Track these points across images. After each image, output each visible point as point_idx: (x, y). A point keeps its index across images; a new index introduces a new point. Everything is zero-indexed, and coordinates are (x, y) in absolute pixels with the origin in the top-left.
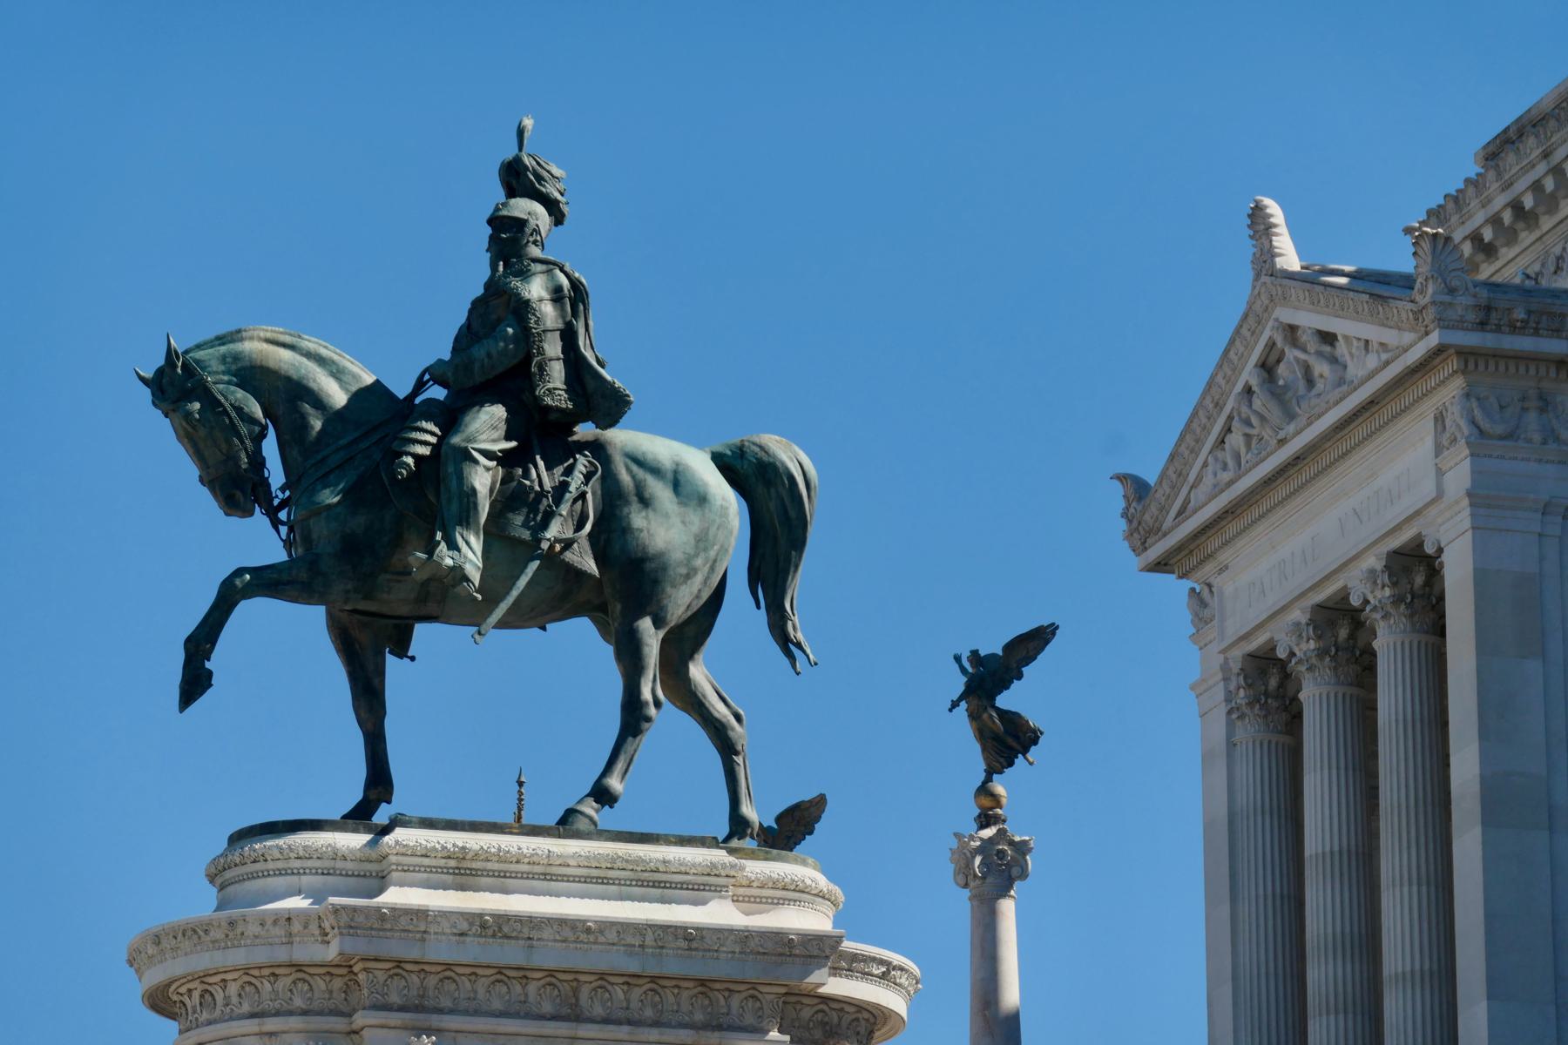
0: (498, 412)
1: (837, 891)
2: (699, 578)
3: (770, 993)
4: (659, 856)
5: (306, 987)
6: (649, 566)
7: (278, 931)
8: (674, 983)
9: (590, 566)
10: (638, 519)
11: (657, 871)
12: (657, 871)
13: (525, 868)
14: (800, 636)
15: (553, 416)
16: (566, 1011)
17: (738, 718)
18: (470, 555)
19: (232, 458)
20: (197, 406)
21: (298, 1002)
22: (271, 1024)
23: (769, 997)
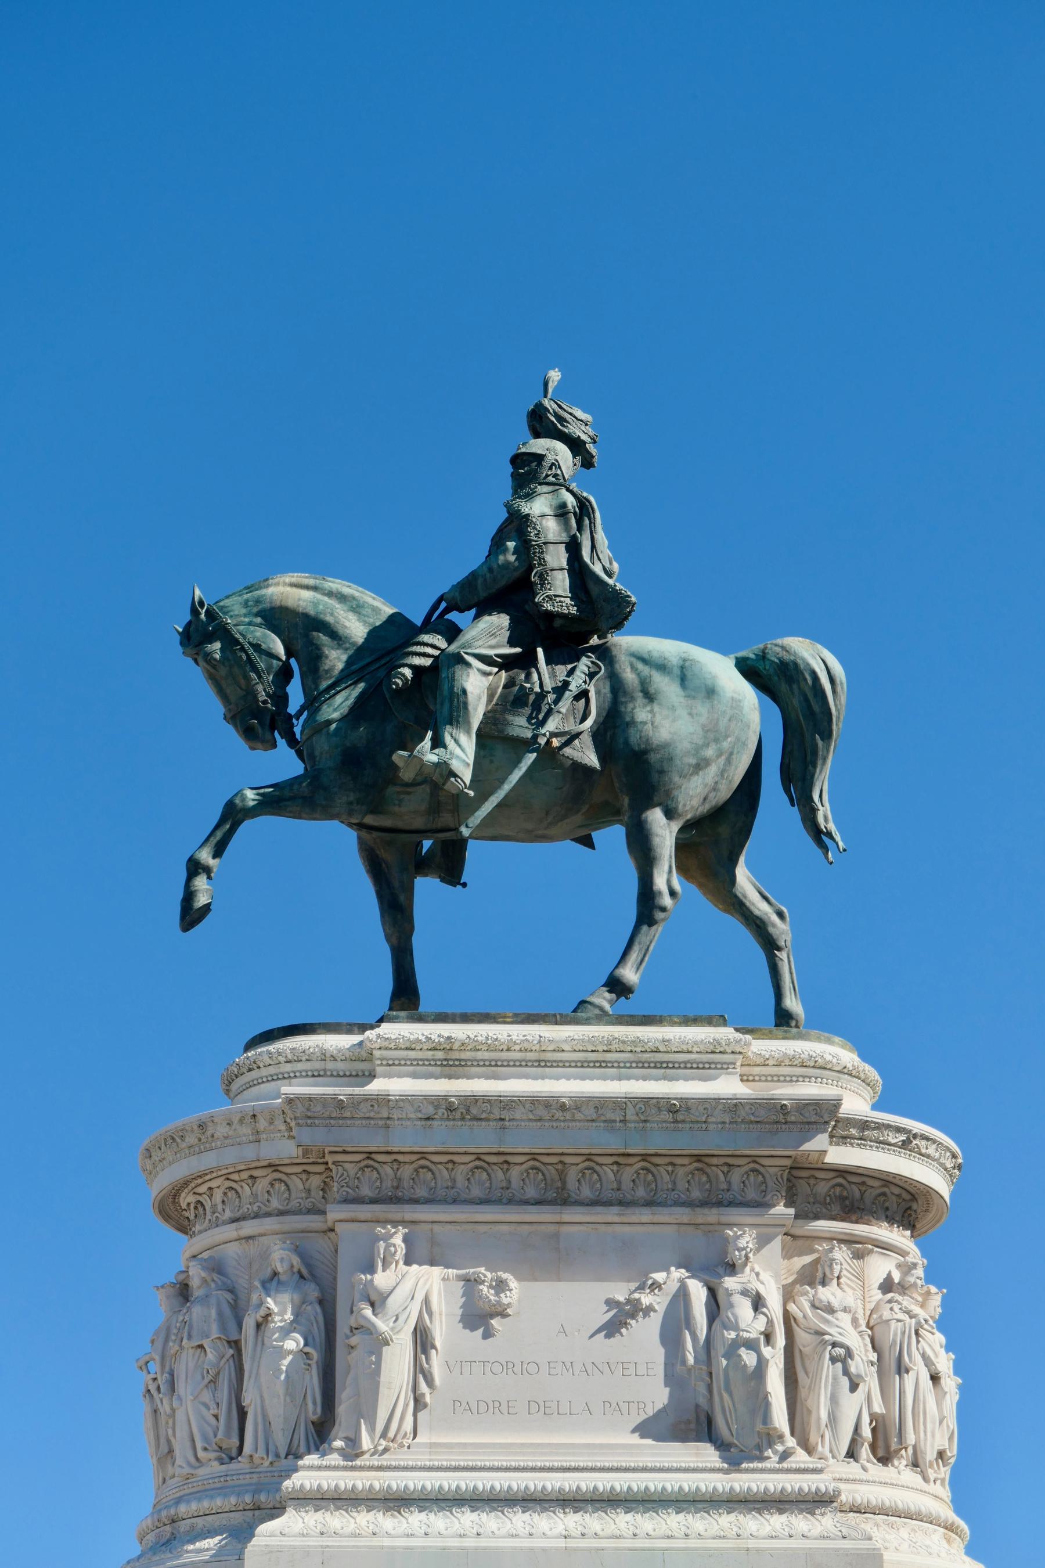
0: (501, 621)
1: (873, 1074)
2: (713, 770)
3: (773, 1169)
4: (660, 1036)
5: (283, 1187)
6: (653, 757)
7: (246, 1130)
8: (667, 1160)
9: (592, 759)
10: (641, 713)
11: (658, 1051)
12: (658, 1051)
13: (518, 1056)
14: (832, 827)
15: (558, 623)
16: (551, 1194)
17: (780, 915)
19: (252, 694)
20: (217, 645)
21: (275, 1204)
22: (249, 1228)
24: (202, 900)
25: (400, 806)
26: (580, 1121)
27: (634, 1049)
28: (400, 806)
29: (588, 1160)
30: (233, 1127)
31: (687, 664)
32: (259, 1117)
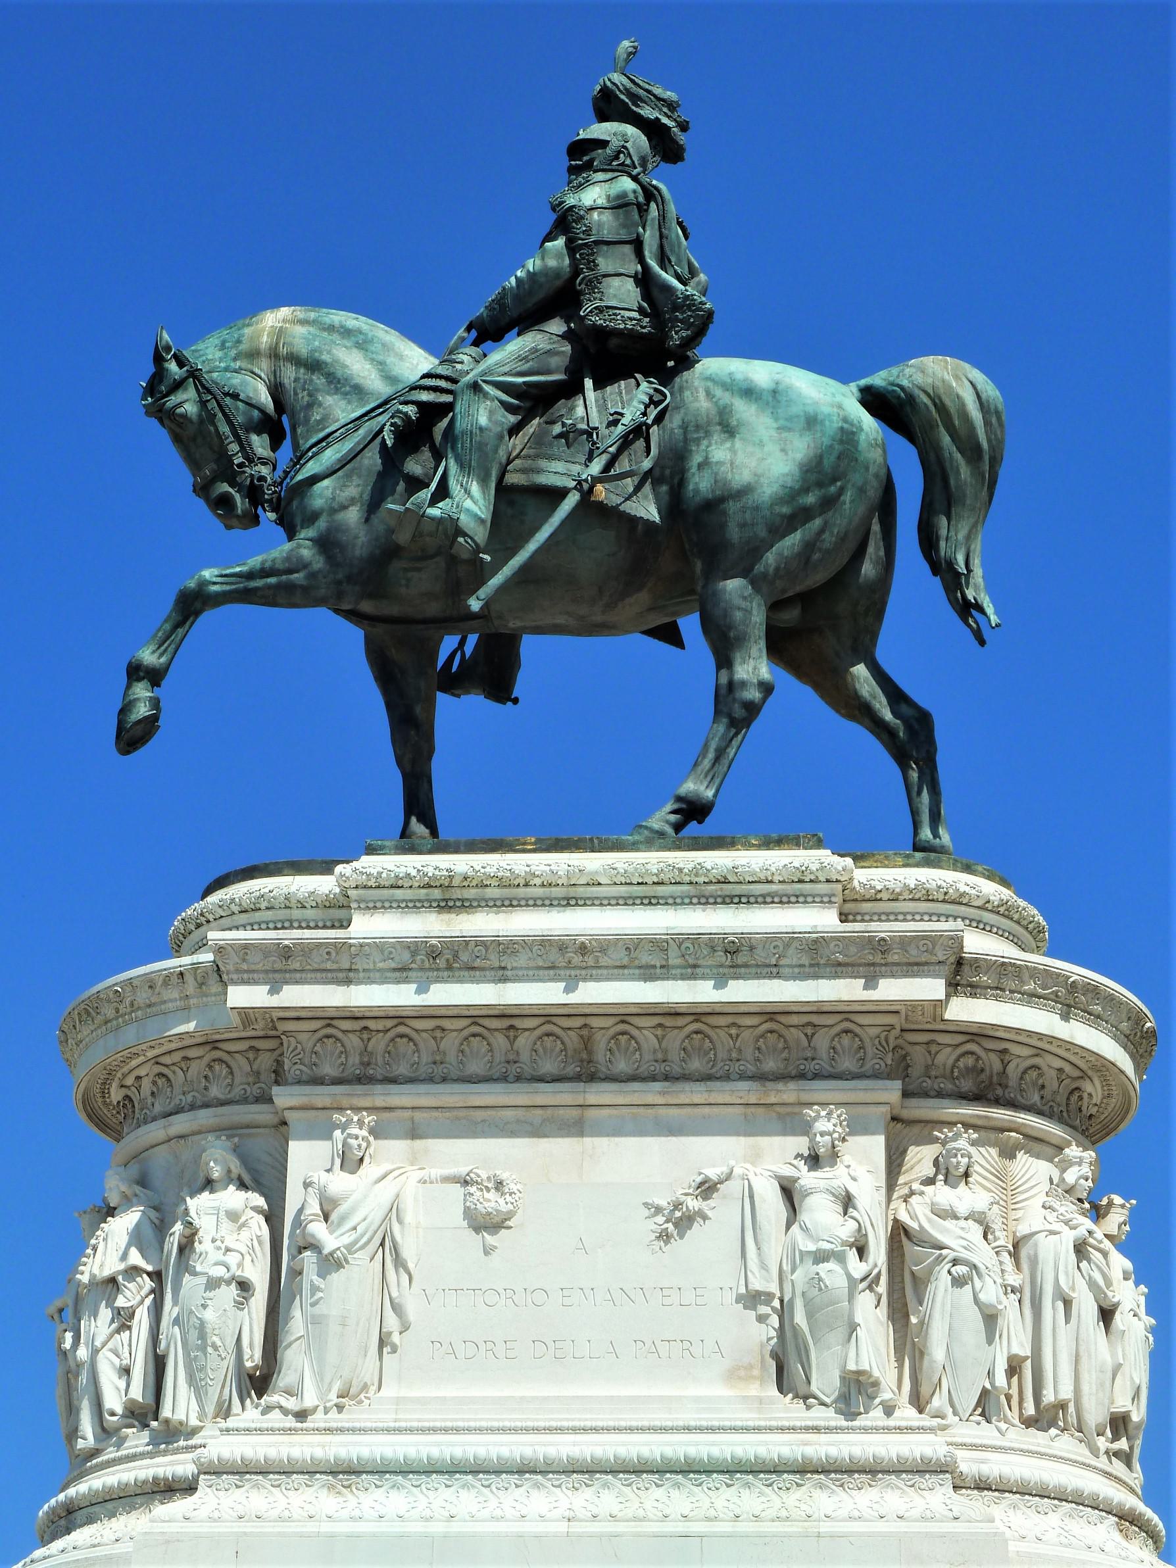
6: (732, 507)
8: (730, 1020)
11: (726, 882)
12: (726, 882)
13: (539, 892)
15: (613, 342)
16: (572, 1069)
18: (468, 504)
23: (873, 1031)
24: (142, 710)
25: (407, 586)
26: (607, 967)
27: (695, 880)
28: (407, 586)
29: (623, 1022)
30: (157, 990)
31: (780, 387)
32: (188, 977)
